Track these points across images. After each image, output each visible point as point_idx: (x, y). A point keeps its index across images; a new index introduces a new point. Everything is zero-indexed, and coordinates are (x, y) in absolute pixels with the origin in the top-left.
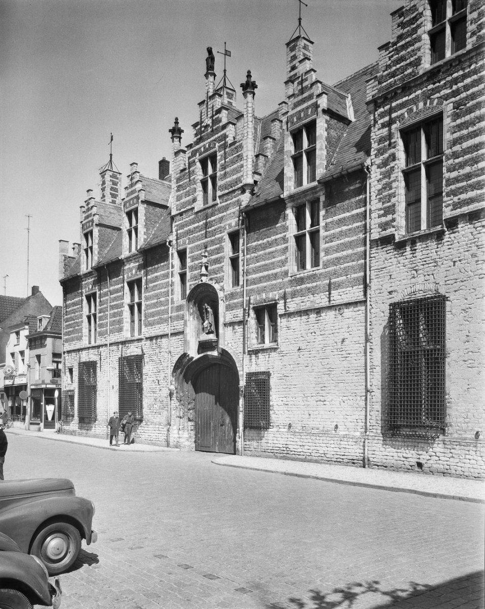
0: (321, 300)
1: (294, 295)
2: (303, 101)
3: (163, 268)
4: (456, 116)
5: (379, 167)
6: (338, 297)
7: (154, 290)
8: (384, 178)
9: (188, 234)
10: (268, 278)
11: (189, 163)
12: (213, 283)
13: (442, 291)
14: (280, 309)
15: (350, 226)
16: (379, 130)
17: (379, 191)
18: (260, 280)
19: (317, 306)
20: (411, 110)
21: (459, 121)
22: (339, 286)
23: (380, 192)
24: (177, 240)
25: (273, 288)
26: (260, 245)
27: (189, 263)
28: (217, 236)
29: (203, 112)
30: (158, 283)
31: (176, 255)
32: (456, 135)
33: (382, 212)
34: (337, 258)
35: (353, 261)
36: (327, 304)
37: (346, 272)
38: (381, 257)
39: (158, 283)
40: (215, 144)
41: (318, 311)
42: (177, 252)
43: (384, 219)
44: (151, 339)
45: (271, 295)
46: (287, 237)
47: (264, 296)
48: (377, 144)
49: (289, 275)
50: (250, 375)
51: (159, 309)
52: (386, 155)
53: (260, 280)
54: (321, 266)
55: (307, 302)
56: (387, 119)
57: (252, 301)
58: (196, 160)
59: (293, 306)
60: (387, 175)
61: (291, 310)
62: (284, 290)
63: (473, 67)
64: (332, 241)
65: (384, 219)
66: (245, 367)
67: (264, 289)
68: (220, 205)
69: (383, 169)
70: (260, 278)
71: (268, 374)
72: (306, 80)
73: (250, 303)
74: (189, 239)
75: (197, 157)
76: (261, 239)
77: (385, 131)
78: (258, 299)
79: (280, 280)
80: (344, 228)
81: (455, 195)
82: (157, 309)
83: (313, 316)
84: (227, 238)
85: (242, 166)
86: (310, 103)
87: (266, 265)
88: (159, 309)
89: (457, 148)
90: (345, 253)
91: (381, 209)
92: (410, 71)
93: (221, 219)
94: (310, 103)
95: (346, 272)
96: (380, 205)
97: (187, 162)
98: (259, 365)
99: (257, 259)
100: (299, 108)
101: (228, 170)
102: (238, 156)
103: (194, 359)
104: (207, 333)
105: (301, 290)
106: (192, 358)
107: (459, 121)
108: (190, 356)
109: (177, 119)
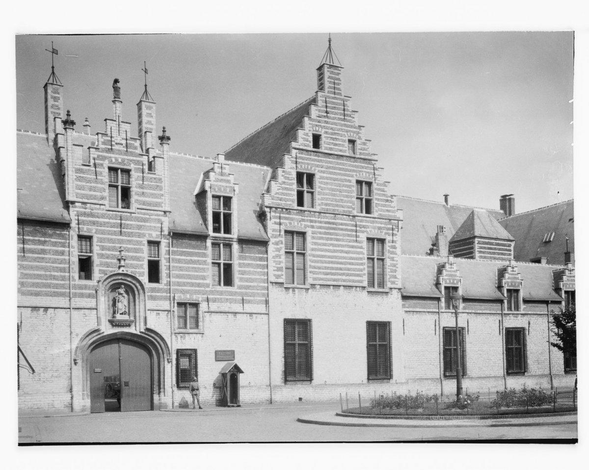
0: (237, 307)
1: (215, 301)
2: (221, 180)
3: (55, 244)
4: (313, 238)
5: (273, 244)
6: (248, 308)
7: (38, 262)
8: (276, 251)
9: (94, 224)
10: (192, 285)
11: (95, 165)
12: (137, 276)
13: (309, 317)
14: (203, 307)
15: (255, 270)
16: (273, 224)
17: (273, 256)
18: (184, 284)
19: (232, 310)
20: (290, 224)
21: (314, 241)
22: (249, 302)
23: (273, 257)
24: (78, 224)
25: (199, 292)
26: (184, 260)
27: (96, 249)
28: (134, 239)
29: (112, 128)
30: (46, 256)
31: (76, 238)
32: (314, 247)
33: (276, 269)
34: (247, 286)
35: (258, 290)
36: (242, 311)
37: (253, 295)
38: (276, 293)
39: (46, 256)
40: (130, 164)
41: (235, 313)
42: (78, 235)
43: (277, 273)
44: (35, 308)
45: (194, 297)
46: (208, 261)
47: (188, 296)
48: (271, 231)
49: (211, 287)
50: (178, 351)
51: (49, 281)
52: (277, 240)
53: (184, 284)
54: (236, 287)
55: (225, 307)
56: (278, 221)
57: (176, 298)
58: (104, 165)
59: (214, 307)
60: (279, 250)
61: (212, 309)
62: (206, 296)
63: (319, 219)
64: (243, 275)
65: (277, 273)
66: (175, 344)
67: (187, 292)
68: (136, 215)
69: (276, 246)
70: (184, 283)
71: (195, 351)
72: (225, 169)
73: (174, 299)
74: (97, 230)
75: (106, 164)
76: (185, 256)
77: (277, 227)
78: (183, 297)
79: (203, 289)
80: (252, 269)
81: (314, 274)
82: (44, 281)
83: (230, 315)
84: (146, 243)
85: (162, 195)
86: (228, 185)
87: (189, 275)
88: (49, 281)
89: (314, 252)
90: (252, 284)
91: (275, 267)
92: (290, 203)
93: (139, 227)
94: (228, 185)
95: (253, 295)
96: (274, 264)
97: (92, 161)
98: (187, 343)
99: (181, 269)
100: (219, 183)
101: (145, 191)
102: (158, 186)
103: (105, 334)
104: (120, 314)
105: (221, 299)
106: (103, 333)
107: (314, 241)
108: (101, 332)
109: (68, 112)
